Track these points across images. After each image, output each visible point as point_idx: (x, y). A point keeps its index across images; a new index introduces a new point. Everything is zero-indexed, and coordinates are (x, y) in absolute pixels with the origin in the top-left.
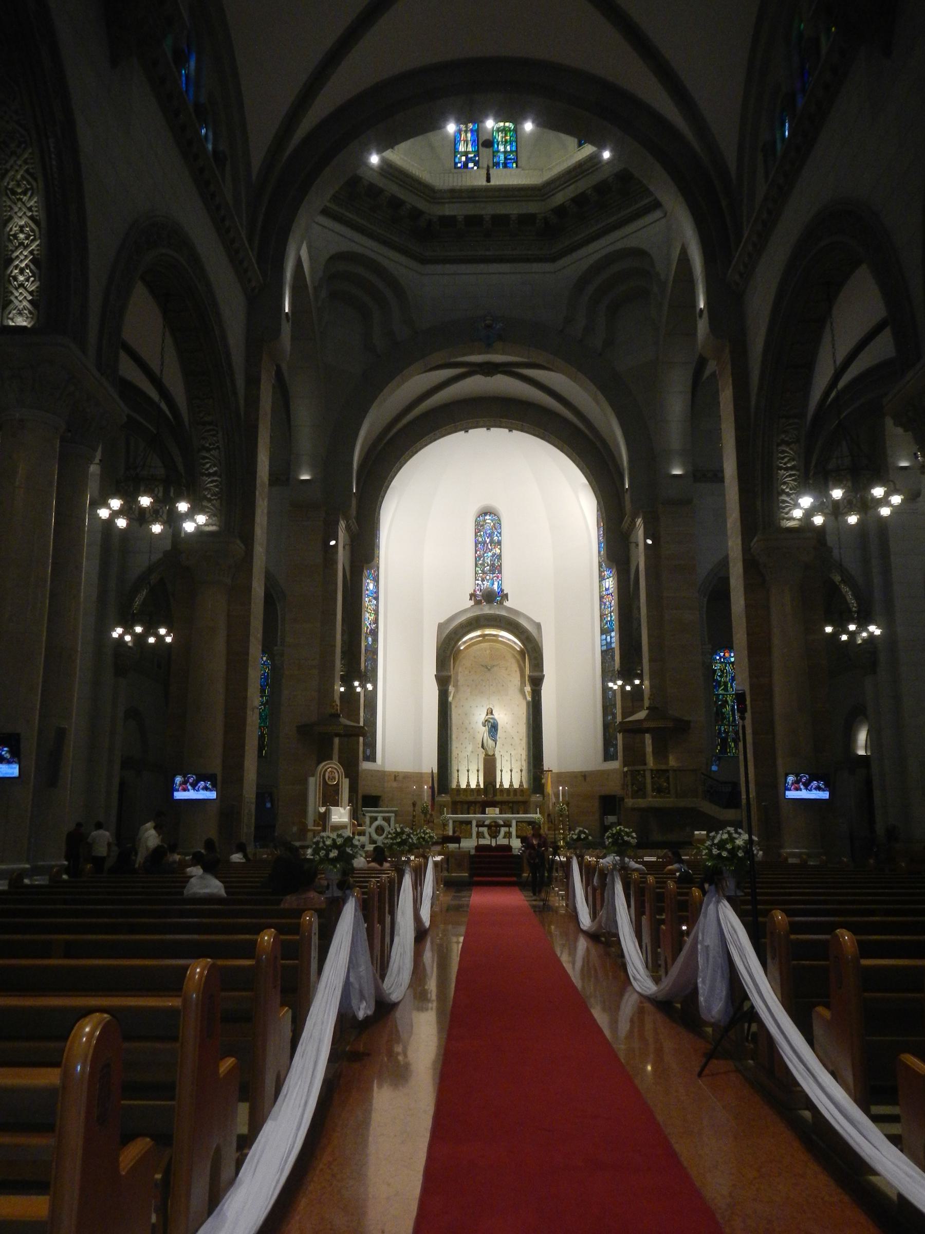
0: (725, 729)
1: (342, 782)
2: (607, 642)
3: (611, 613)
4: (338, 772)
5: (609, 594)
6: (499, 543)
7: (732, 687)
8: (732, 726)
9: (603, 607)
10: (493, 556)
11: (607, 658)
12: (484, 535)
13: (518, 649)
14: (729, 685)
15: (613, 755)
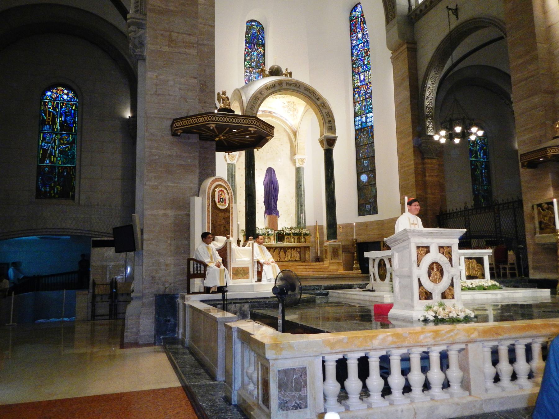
0: (477, 188)
1: (232, 208)
2: (362, 123)
3: (366, 99)
4: (228, 192)
5: (364, 84)
6: (263, 45)
7: (480, 155)
8: (482, 185)
9: (357, 95)
10: (258, 54)
11: (362, 135)
12: (251, 37)
13: (290, 125)
14: (478, 154)
15: (370, 210)
